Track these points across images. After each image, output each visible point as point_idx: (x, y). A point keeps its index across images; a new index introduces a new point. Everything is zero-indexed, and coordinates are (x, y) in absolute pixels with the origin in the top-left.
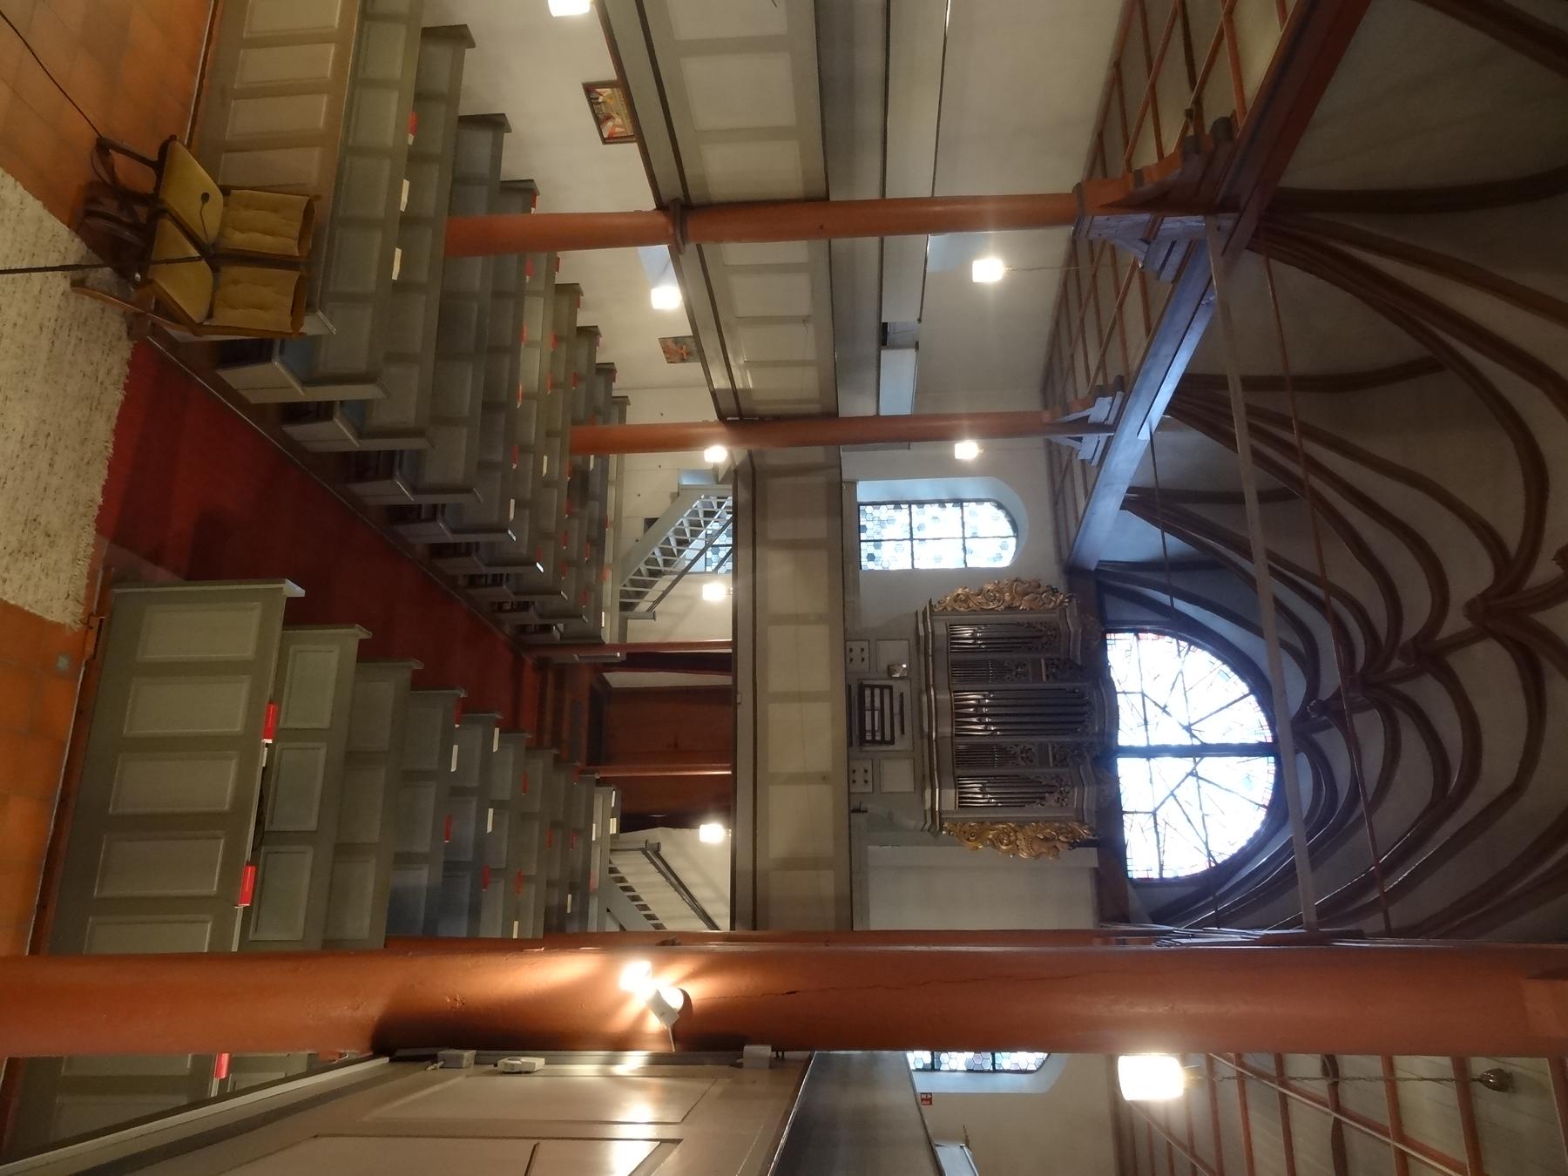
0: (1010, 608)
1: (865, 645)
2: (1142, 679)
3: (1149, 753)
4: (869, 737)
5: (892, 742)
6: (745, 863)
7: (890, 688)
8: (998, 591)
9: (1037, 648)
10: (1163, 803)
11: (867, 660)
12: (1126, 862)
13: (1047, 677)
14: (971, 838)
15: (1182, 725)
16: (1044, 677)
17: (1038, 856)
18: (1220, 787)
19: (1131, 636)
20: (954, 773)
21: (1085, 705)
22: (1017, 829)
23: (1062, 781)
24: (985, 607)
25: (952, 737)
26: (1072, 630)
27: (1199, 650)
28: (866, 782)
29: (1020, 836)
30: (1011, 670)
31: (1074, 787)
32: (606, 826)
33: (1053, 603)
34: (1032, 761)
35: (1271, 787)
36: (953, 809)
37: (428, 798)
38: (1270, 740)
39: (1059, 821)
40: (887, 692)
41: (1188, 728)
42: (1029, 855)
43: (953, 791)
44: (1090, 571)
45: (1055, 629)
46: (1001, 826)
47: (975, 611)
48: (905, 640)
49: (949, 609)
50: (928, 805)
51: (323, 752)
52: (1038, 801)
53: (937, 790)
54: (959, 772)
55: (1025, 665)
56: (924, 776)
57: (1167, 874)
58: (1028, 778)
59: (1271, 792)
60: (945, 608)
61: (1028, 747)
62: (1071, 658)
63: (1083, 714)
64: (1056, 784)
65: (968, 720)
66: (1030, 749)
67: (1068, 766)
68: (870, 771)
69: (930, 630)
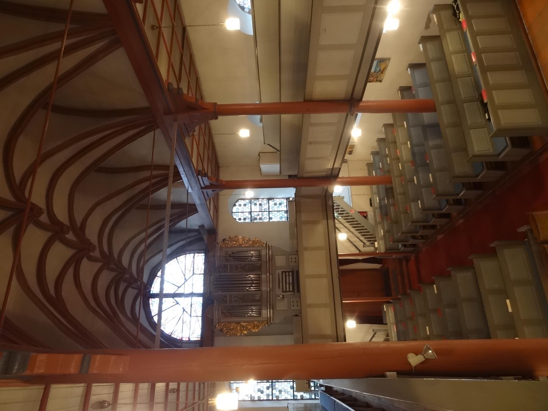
2: (190, 322)
3: (192, 295)
4: (291, 274)
5: (282, 272)
6: (331, 222)
7: (283, 292)
8: (242, 330)
10: (190, 278)
11: (292, 302)
12: (205, 258)
13: (227, 296)
15: (179, 305)
17: (236, 236)
18: (170, 283)
19: (192, 339)
20: (262, 262)
21: (216, 284)
23: (226, 259)
24: (247, 323)
25: (262, 274)
26: (217, 311)
27: (168, 333)
28: (291, 258)
29: (241, 243)
30: (240, 298)
31: (222, 256)
32: (379, 244)
33: (222, 325)
34: (235, 266)
35: (154, 283)
36: (262, 250)
37: (436, 164)
38: (150, 299)
39: (228, 247)
40: (284, 290)
41: (178, 303)
42: (238, 237)
43: (262, 254)
45: (223, 313)
46: (247, 245)
47: (251, 322)
48: (278, 310)
49: (261, 322)
50: (270, 251)
51: (469, 122)
52: (234, 253)
53: (267, 253)
54: (260, 262)
55: (235, 301)
56: (272, 260)
57: (192, 255)
59: (154, 281)
60: (262, 323)
62: (218, 303)
63: (216, 281)
64: (228, 257)
67: (223, 265)
68: (290, 262)
69: (268, 310)
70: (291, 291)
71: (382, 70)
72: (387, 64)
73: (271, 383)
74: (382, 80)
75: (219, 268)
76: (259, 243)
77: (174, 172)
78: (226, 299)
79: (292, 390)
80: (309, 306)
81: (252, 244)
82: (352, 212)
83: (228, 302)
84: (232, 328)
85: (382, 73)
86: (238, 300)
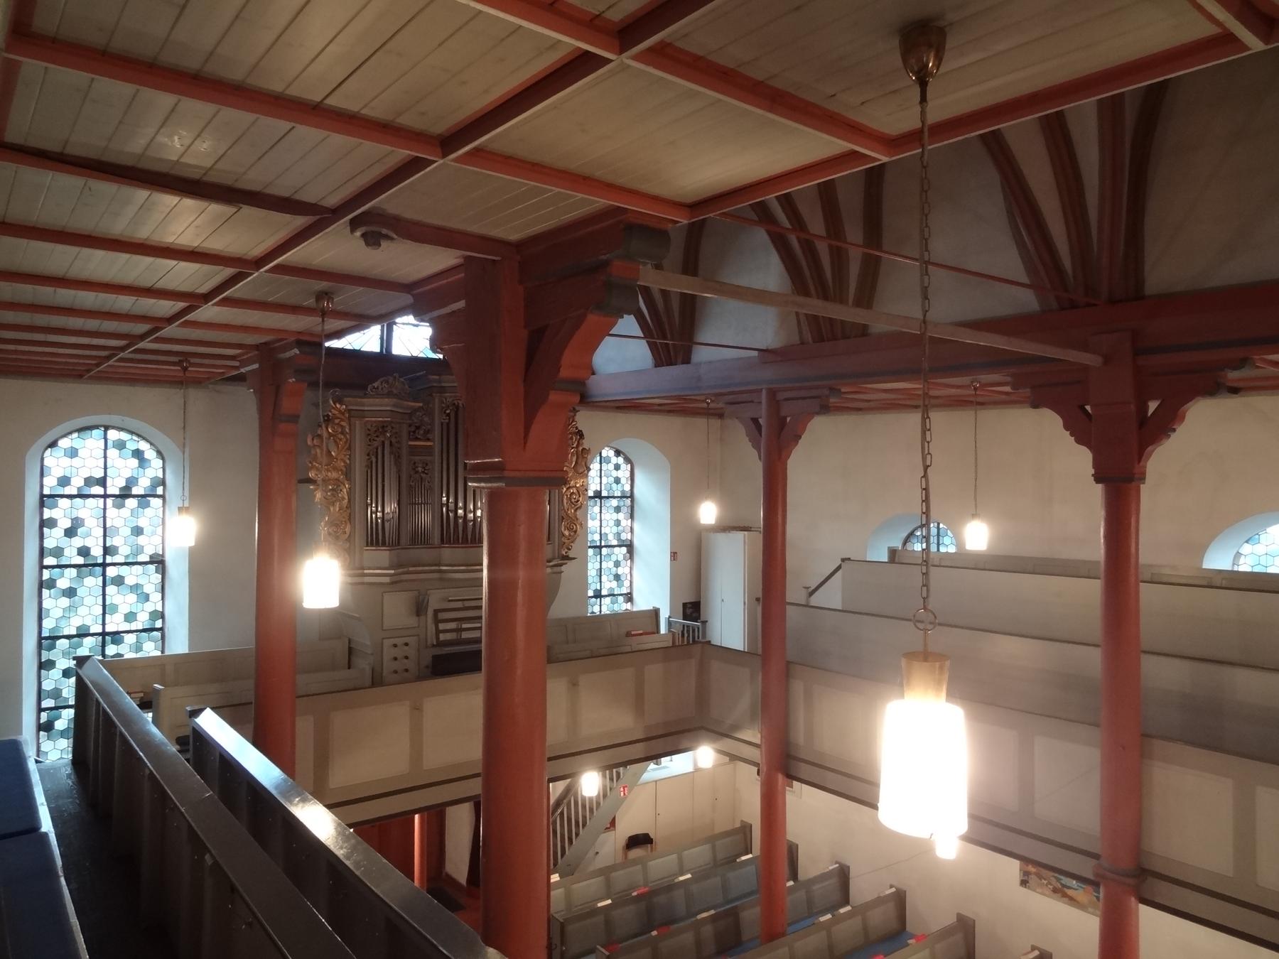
0: (348, 474)
1: (387, 643)
7: (436, 612)
13: (428, 440)
16: (429, 443)
22: (568, 486)
24: (346, 501)
33: (343, 423)
40: (442, 616)
46: (565, 501)
55: (415, 463)
62: (409, 412)
65: (461, 528)
70: (438, 638)
71: (1069, 892)
72: (1090, 910)
73: (100, 561)
74: (1029, 888)
76: (570, 535)
77: (845, 321)
79: (75, 633)
80: (417, 709)
81: (567, 515)
82: (622, 789)
84: (333, 453)
85: (1055, 891)
86: (417, 472)
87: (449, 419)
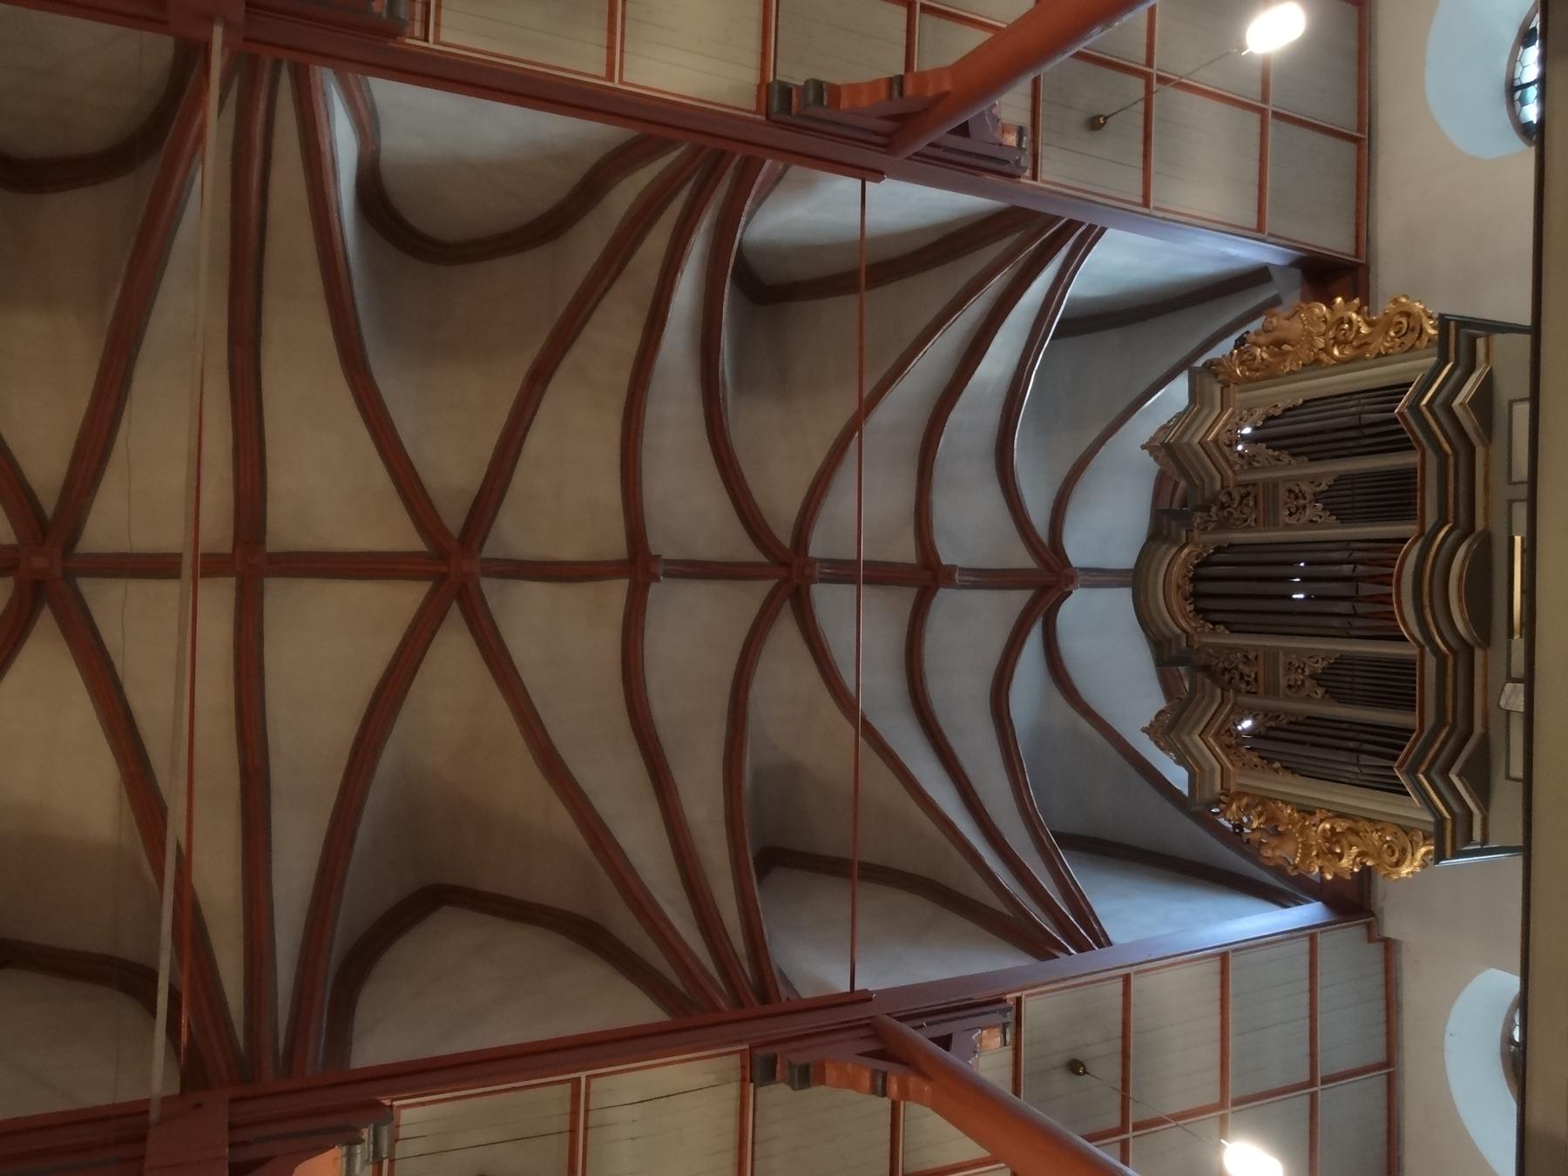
9: (1266, 715)
13: (1256, 657)
14: (1404, 320)
30: (1311, 676)
31: (1216, 441)
34: (1290, 491)
44: (1324, 902)
58: (1294, 455)
61: (1292, 521)
62: (1219, 691)
66: (1291, 514)
67: (1239, 485)
75: (1223, 506)
78: (1253, 676)
83: (1262, 686)
87: (1220, 623)
